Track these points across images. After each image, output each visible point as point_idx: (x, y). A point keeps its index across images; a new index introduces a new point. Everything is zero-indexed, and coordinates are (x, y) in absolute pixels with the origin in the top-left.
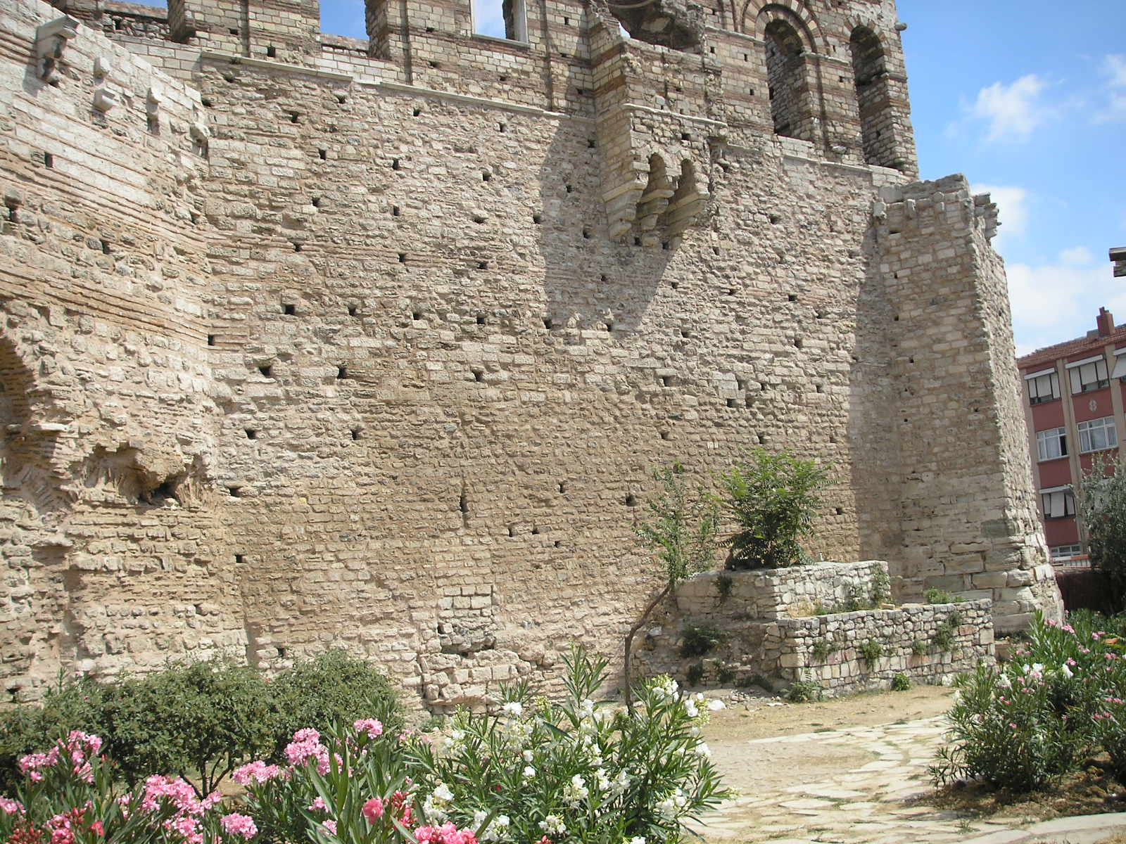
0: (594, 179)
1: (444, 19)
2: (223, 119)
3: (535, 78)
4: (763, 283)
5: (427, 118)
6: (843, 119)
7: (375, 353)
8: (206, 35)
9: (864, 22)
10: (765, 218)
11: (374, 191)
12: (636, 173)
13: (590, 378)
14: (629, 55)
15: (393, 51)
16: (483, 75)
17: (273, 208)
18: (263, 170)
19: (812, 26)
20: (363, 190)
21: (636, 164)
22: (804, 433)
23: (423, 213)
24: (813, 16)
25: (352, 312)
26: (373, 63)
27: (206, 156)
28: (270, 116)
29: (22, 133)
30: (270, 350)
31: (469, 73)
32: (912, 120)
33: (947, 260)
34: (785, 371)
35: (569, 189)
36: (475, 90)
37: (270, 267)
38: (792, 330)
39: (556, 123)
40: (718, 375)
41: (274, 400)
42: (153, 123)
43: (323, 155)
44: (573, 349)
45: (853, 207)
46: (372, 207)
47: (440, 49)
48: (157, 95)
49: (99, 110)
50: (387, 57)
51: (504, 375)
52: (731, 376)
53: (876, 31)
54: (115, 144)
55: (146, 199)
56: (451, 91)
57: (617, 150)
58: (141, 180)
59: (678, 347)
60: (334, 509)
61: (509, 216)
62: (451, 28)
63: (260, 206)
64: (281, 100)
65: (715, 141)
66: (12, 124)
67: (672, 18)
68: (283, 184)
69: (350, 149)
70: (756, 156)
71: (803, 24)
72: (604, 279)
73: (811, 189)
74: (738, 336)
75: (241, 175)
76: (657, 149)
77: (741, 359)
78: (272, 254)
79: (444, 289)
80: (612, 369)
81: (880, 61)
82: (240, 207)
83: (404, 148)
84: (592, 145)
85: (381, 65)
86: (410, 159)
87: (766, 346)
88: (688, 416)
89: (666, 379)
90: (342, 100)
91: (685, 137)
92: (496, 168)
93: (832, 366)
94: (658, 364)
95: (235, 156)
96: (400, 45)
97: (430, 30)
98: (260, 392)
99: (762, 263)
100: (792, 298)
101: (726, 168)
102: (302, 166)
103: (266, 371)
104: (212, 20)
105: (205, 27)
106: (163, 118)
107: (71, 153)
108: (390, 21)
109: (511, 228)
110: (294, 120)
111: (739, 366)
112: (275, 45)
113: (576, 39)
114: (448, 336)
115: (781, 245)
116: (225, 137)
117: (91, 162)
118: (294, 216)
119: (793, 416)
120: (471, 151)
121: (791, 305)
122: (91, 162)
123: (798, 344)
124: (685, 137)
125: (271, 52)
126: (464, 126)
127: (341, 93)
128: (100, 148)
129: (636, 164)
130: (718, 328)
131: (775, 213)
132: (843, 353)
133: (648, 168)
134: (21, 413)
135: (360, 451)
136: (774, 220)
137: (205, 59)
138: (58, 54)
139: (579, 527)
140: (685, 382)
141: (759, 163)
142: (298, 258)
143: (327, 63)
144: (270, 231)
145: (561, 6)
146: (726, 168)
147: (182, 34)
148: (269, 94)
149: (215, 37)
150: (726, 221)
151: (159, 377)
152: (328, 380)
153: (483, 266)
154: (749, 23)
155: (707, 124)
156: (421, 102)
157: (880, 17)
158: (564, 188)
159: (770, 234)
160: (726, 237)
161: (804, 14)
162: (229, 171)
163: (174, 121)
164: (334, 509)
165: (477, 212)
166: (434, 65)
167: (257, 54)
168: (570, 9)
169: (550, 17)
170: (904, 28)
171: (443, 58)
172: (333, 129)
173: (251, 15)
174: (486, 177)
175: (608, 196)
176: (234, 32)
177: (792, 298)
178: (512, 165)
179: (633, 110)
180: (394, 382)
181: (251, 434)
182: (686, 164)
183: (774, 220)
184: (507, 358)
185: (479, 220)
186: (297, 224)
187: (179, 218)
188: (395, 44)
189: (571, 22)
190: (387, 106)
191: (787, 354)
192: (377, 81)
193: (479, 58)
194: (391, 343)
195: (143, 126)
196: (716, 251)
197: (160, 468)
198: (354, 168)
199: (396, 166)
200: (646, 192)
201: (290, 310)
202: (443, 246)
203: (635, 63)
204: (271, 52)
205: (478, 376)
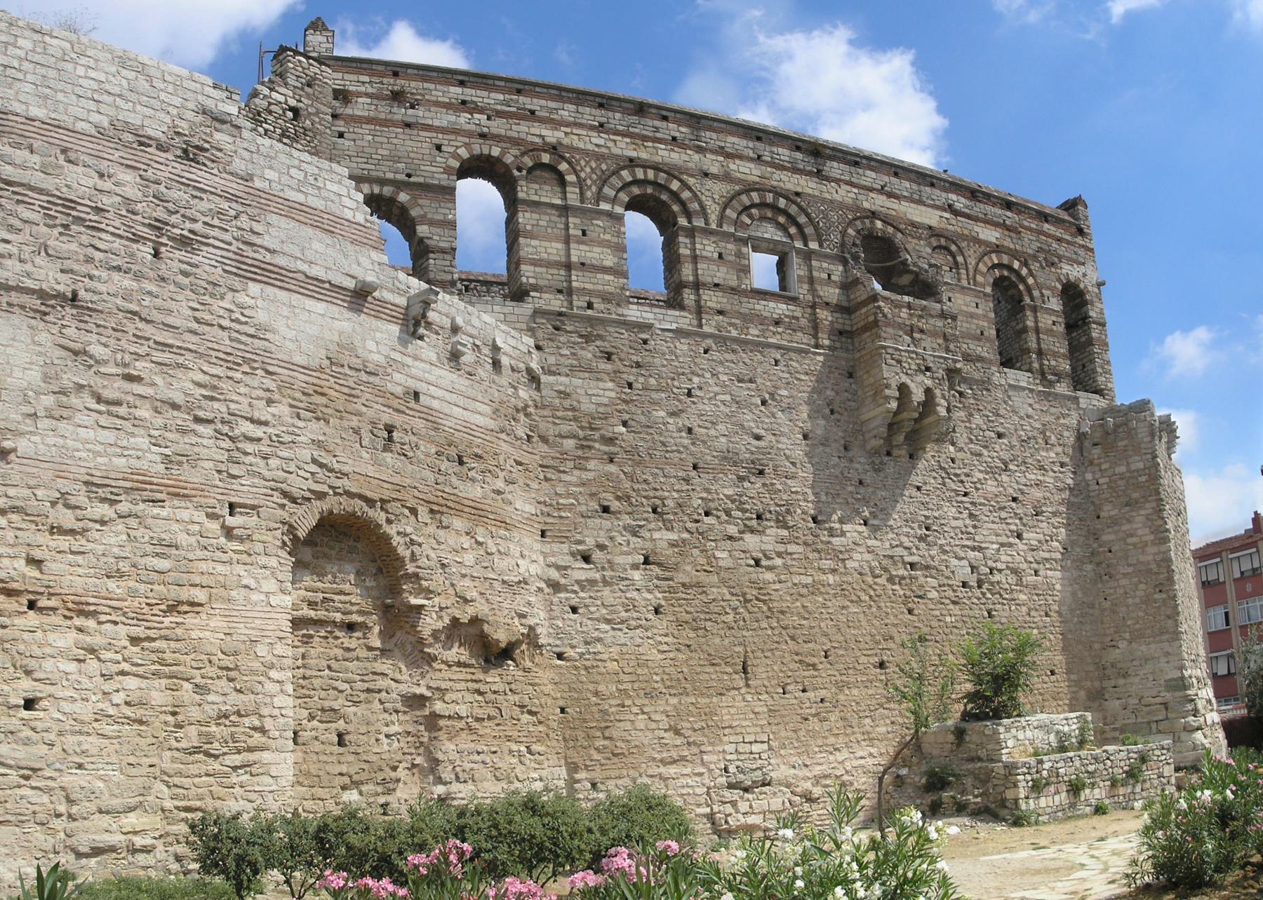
0: (853, 404)
1: (728, 277)
2: (552, 360)
3: (803, 322)
5: (715, 355)
8: (538, 295)
10: (992, 435)
11: (672, 414)
12: (887, 398)
14: (881, 304)
15: (686, 302)
16: (761, 320)
17: (592, 429)
20: (662, 414)
21: (887, 392)
22: (1024, 609)
23: (712, 432)
26: (670, 312)
27: (538, 389)
28: (590, 356)
31: (749, 318)
34: (1009, 559)
35: (832, 412)
38: (1015, 525)
39: (821, 358)
40: (954, 562)
42: (496, 364)
43: (630, 385)
46: (670, 427)
47: (725, 300)
48: (499, 343)
49: (455, 356)
50: (682, 307)
52: (965, 563)
54: (467, 383)
55: (492, 424)
56: (734, 333)
57: (872, 380)
58: (487, 410)
59: (922, 539)
61: (782, 434)
62: (734, 283)
63: (582, 428)
64: (598, 343)
65: (952, 373)
66: (389, 370)
68: (601, 410)
72: (861, 483)
74: (971, 530)
75: (567, 403)
76: (905, 379)
77: (973, 549)
82: (565, 428)
83: (696, 379)
84: (851, 375)
85: (677, 313)
86: (701, 389)
87: (994, 538)
88: (930, 595)
89: (912, 565)
90: (645, 342)
91: (928, 369)
92: (772, 395)
93: (1046, 555)
94: (905, 553)
95: (562, 388)
96: (692, 297)
97: (716, 285)
99: (991, 471)
100: (1014, 500)
101: (961, 394)
102: (613, 395)
104: (541, 283)
105: (536, 288)
106: (505, 361)
108: (684, 278)
109: (785, 443)
110: (609, 359)
111: (971, 554)
112: (593, 300)
113: (837, 291)
115: (1006, 456)
117: (448, 396)
119: (1015, 595)
120: (751, 381)
121: (1014, 505)
122: (448, 396)
123: (1019, 536)
124: (928, 369)
125: (590, 306)
126: (744, 361)
127: (644, 336)
128: (456, 386)
129: (887, 392)
131: (1000, 429)
132: (1055, 544)
133: (897, 394)
136: (1000, 436)
137: (537, 313)
138: (424, 316)
140: (927, 567)
141: (988, 390)
143: (634, 313)
144: (590, 447)
145: (825, 265)
146: (961, 394)
147: (519, 295)
148: (588, 338)
149: (544, 295)
150: (961, 437)
155: (945, 359)
158: (827, 411)
159: (997, 447)
160: (961, 449)
162: (557, 401)
163: (513, 362)
165: (756, 431)
166: (720, 312)
167: (578, 308)
168: (832, 267)
169: (815, 274)
171: (728, 307)
172: (638, 365)
173: (574, 278)
174: (764, 403)
175: (864, 417)
176: (560, 291)
177: (1014, 500)
178: (784, 393)
179: (885, 347)
182: (928, 391)
183: (1000, 436)
185: (758, 438)
186: (610, 441)
187: (518, 439)
188: (689, 297)
189: (833, 277)
190: (683, 346)
191: (1010, 545)
192: (674, 326)
193: (757, 307)
195: (489, 367)
196: (953, 460)
198: (655, 395)
199: (689, 394)
200: (896, 413)
203: (886, 310)
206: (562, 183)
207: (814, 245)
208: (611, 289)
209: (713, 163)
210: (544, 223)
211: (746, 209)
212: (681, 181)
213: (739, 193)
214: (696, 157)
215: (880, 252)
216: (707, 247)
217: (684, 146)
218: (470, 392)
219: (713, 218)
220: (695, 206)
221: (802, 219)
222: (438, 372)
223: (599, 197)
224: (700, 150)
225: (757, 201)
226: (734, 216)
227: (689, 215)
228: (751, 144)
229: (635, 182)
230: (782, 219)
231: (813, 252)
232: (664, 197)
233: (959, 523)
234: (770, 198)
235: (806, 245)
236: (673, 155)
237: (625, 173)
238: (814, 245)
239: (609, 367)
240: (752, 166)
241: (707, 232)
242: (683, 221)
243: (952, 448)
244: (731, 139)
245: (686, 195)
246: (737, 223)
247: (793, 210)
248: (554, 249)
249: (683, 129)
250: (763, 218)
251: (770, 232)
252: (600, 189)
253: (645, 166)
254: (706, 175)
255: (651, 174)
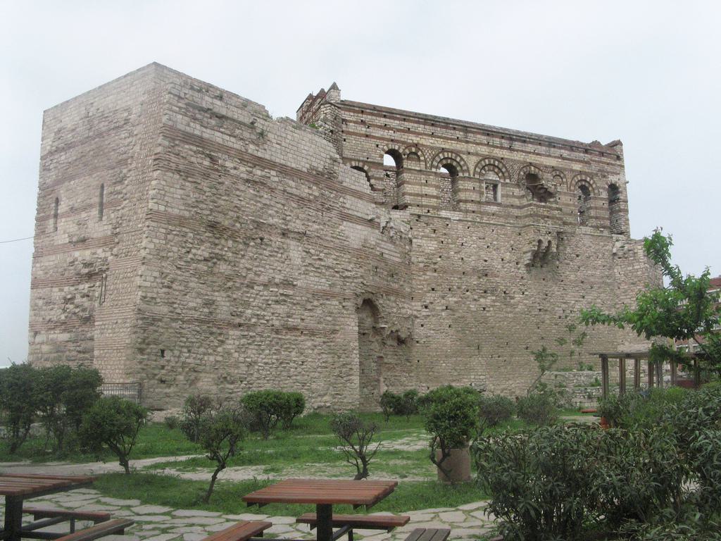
2: (416, 233)
4: (572, 277)
6: (604, 218)
7: (456, 302)
9: (613, 182)
10: (574, 255)
13: (517, 310)
18: (426, 248)
19: (594, 186)
20: (453, 253)
24: (594, 182)
25: (450, 290)
29: (378, 249)
30: (428, 301)
32: (630, 216)
33: (637, 269)
35: (512, 249)
36: (485, 219)
37: (428, 277)
39: (509, 228)
40: (557, 308)
41: (429, 316)
43: (442, 242)
44: (512, 301)
45: (605, 250)
51: (491, 309)
52: (561, 309)
53: (617, 185)
56: (478, 220)
60: (444, 348)
62: (479, 200)
67: (546, 189)
69: (450, 240)
70: (573, 234)
71: (591, 185)
73: (591, 245)
76: (541, 238)
77: (565, 303)
78: (428, 273)
79: (475, 283)
80: (523, 307)
81: (618, 195)
82: (420, 259)
84: (520, 234)
89: (540, 310)
90: (448, 225)
91: (550, 233)
98: (424, 314)
99: (573, 270)
103: (426, 307)
104: (412, 202)
105: (410, 205)
107: (387, 252)
111: (563, 305)
114: (476, 297)
116: (416, 238)
118: (434, 261)
120: (484, 239)
121: (582, 284)
123: (583, 297)
124: (550, 233)
125: (429, 211)
130: (557, 293)
131: (578, 253)
134: (376, 322)
135: (451, 331)
136: (578, 256)
137: (412, 214)
139: (512, 356)
140: (546, 310)
142: (435, 274)
151: (403, 311)
152: (443, 310)
153: (486, 275)
154: (572, 188)
156: (470, 223)
157: (619, 180)
161: (591, 182)
164: (444, 348)
166: (473, 212)
170: (628, 182)
172: (445, 234)
174: (488, 247)
176: (418, 206)
177: (582, 282)
180: (461, 311)
181: (422, 326)
182: (549, 242)
183: (578, 256)
184: (493, 304)
185: (486, 261)
186: (435, 263)
189: (515, 194)
192: (458, 219)
194: (460, 299)
197: (403, 336)
198: (450, 246)
199: (462, 245)
201: (433, 289)
202: (474, 270)
204: (429, 211)
205: (484, 309)
206: (419, 160)
207: (508, 181)
208: (435, 205)
209: (472, 148)
210: (412, 178)
211: (484, 167)
212: (460, 157)
213: (481, 160)
214: (465, 145)
215: (534, 185)
216: (469, 185)
217: (461, 141)
218: (394, 250)
219: (472, 172)
220: (465, 168)
221: (504, 170)
222: (388, 244)
223: (432, 166)
224: (467, 142)
225: (487, 163)
226: (479, 171)
227: (463, 171)
228: (485, 138)
229: (445, 158)
230: (496, 170)
231: (507, 183)
232: (454, 164)
233: (559, 293)
234: (492, 162)
235: (505, 180)
236: (458, 146)
237: (441, 155)
238: (508, 181)
239: (434, 235)
240: (485, 147)
241: (469, 178)
242: (461, 174)
243: (558, 262)
244: (479, 136)
245: (462, 163)
246: (480, 174)
247: (500, 166)
248: (416, 189)
249: (461, 133)
250: (489, 170)
251: (492, 176)
252: (432, 162)
253: (448, 151)
254: (469, 153)
255: (450, 154)
